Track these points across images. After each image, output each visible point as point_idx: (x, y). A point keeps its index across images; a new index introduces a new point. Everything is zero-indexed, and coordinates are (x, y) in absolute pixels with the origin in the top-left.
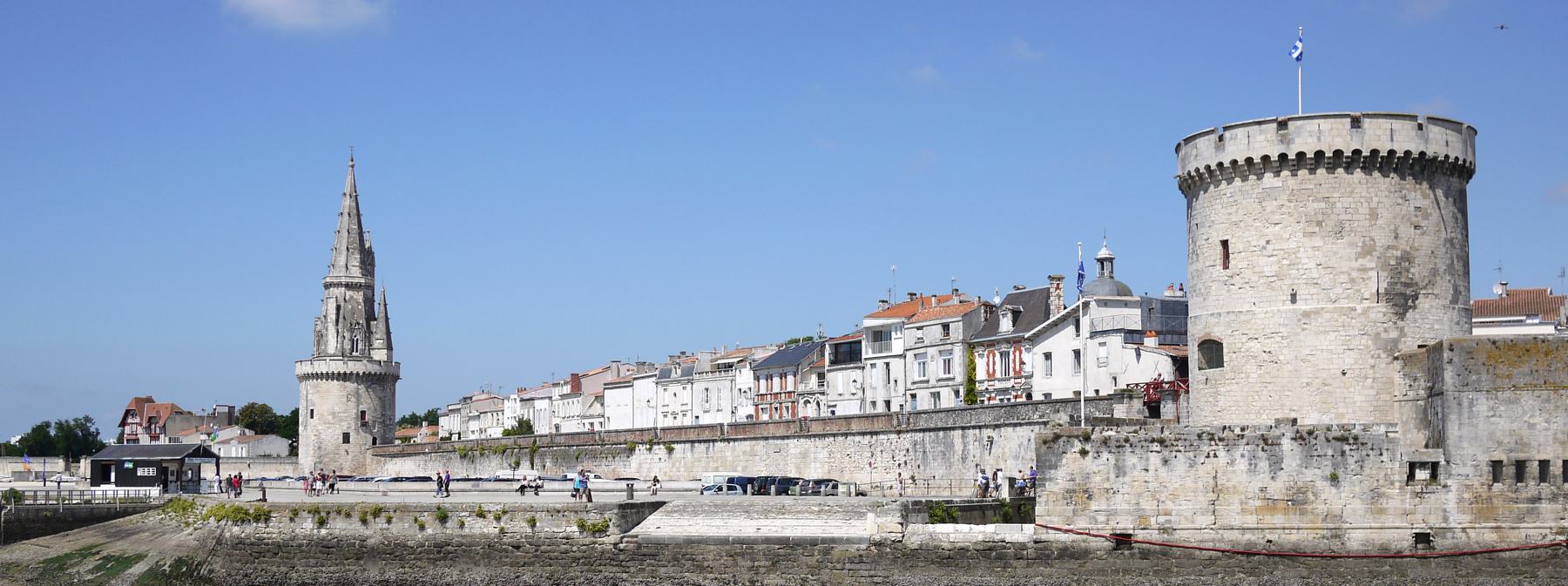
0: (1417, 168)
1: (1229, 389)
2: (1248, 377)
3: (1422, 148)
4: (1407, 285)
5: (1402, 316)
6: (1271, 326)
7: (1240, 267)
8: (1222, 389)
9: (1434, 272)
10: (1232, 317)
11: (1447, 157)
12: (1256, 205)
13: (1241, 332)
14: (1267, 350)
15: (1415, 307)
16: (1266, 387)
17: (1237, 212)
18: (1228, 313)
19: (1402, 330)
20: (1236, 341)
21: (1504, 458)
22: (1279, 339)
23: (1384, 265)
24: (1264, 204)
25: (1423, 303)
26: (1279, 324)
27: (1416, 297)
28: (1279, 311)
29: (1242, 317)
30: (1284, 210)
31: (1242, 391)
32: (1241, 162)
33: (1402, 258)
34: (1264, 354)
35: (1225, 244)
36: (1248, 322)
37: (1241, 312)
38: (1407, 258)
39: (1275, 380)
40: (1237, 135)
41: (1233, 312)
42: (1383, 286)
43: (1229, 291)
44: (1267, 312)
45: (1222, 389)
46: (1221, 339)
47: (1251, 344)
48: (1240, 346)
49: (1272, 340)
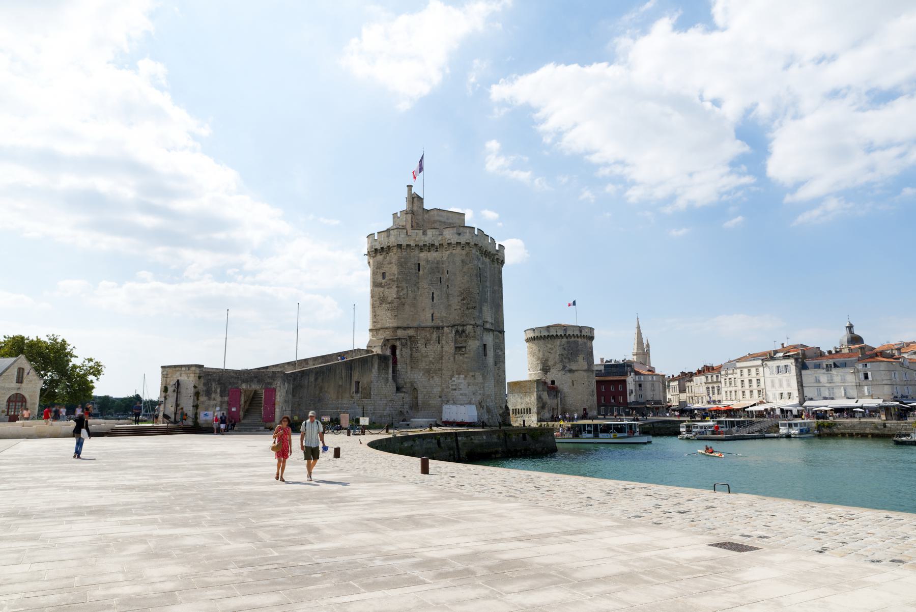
0: (549, 338)
3: (548, 334)
4: (546, 367)
5: (546, 374)
9: (555, 363)
11: (557, 335)
15: (550, 371)
19: (546, 377)
21: (513, 408)
23: (542, 363)
25: (552, 370)
27: (550, 369)
33: (546, 360)
38: (547, 360)
42: (541, 367)
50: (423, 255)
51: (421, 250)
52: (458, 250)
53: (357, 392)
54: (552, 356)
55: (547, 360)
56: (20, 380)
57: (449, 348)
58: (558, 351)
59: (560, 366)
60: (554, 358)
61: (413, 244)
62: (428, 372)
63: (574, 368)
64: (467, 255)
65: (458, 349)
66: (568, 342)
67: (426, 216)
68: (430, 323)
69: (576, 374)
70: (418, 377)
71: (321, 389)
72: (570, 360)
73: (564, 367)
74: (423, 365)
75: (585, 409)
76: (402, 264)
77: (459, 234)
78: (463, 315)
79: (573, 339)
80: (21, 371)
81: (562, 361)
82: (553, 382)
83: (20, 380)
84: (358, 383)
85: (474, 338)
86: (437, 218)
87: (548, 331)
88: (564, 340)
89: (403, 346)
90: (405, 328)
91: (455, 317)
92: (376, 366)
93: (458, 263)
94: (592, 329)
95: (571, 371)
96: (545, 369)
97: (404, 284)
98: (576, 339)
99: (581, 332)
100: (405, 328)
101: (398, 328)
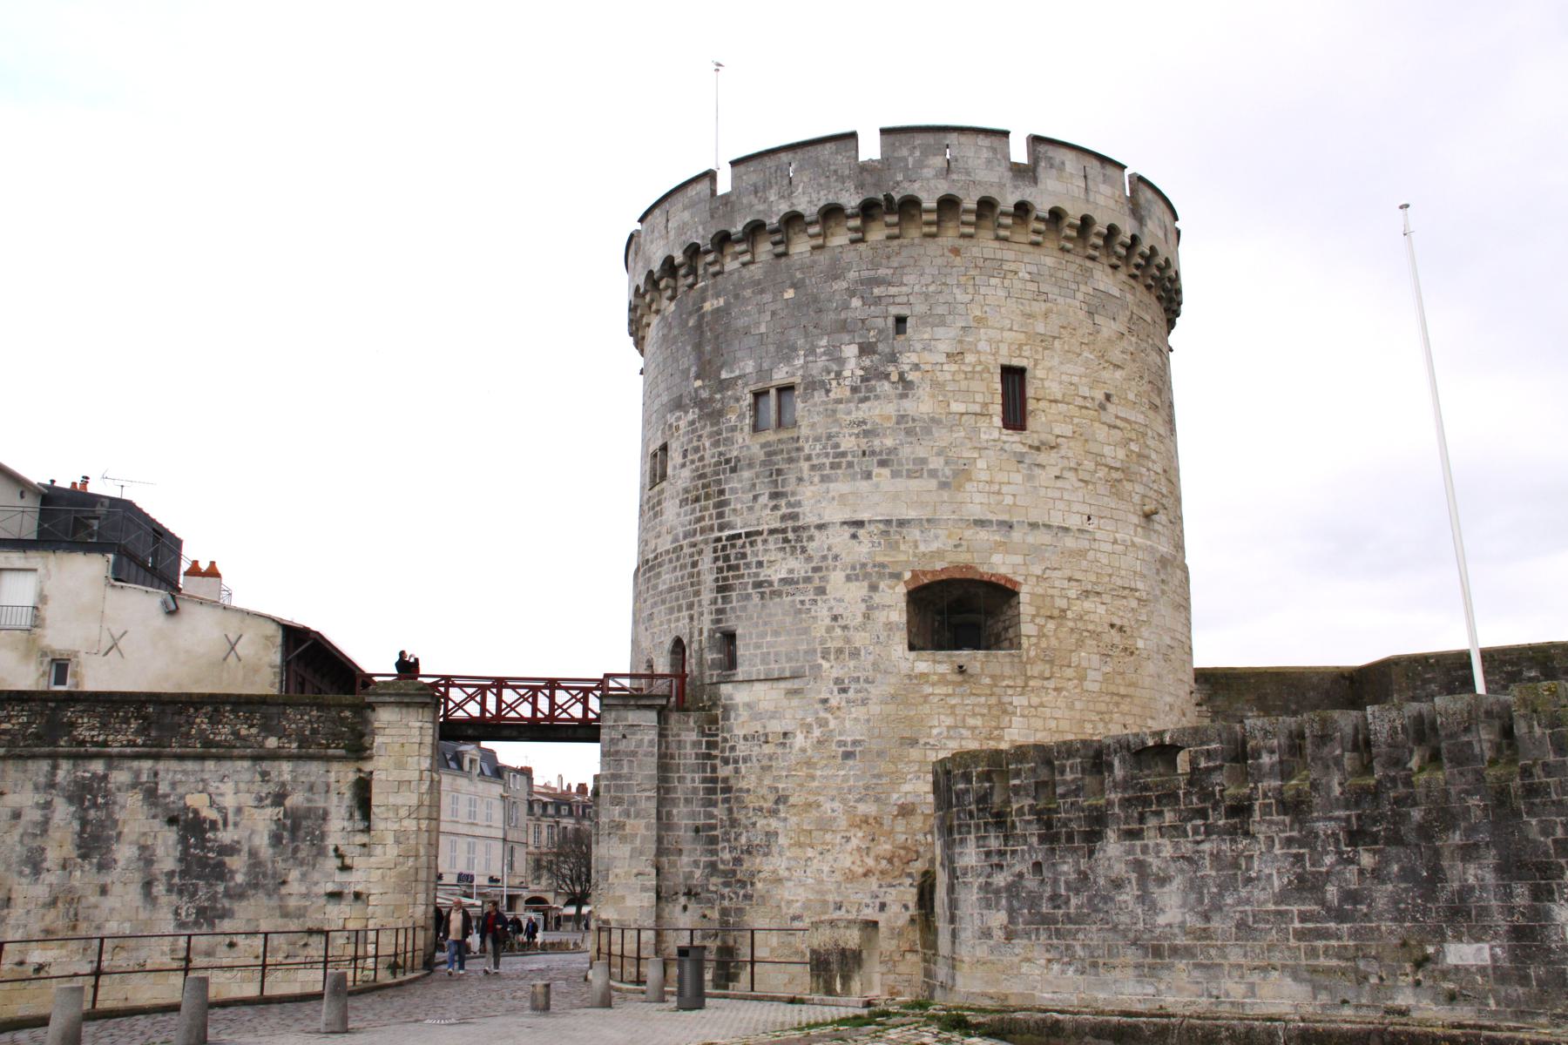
1: (1035, 700)
2: (1082, 678)
6: (1123, 573)
7: (1057, 431)
8: (1016, 701)
10: (1043, 537)
12: (1082, 315)
13: (1068, 573)
14: (1118, 622)
16: (1117, 704)
17: (1046, 315)
18: (1034, 526)
20: (1056, 592)
22: (1134, 604)
24: (1098, 319)
26: (1135, 572)
28: (1133, 544)
29: (1069, 542)
30: (1124, 344)
31: (1071, 707)
32: (1074, 213)
34: (1113, 632)
35: (1013, 377)
36: (1082, 553)
37: (1067, 530)
39: (1131, 690)
40: (1063, 163)
41: (1048, 526)
43: (1030, 478)
44: (1115, 542)
45: (1016, 701)
46: (1016, 583)
47: (1088, 605)
48: (1063, 603)
49: (1124, 602)
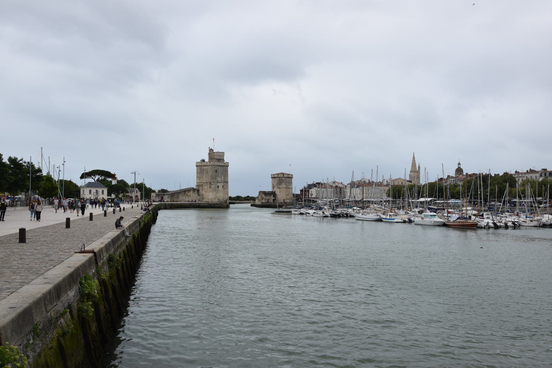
50: (204, 167)
51: (204, 166)
52: (210, 167)
53: (187, 196)
54: (275, 183)
55: (274, 185)
56: (137, 193)
57: (209, 187)
58: (276, 182)
59: (277, 186)
60: (275, 184)
61: (202, 165)
62: (205, 191)
63: (281, 187)
64: (212, 167)
65: (210, 187)
66: (279, 179)
67: (214, 154)
68: (205, 182)
69: (281, 189)
70: (203, 193)
71: (178, 195)
72: (279, 185)
73: (278, 187)
74: (204, 190)
75: (284, 200)
76: (200, 169)
77: (210, 163)
78: (211, 180)
79: (281, 178)
80: (137, 191)
81: (277, 185)
82: (275, 191)
83: (137, 193)
84: (187, 194)
85: (213, 185)
86: (217, 154)
87: (274, 175)
88: (278, 178)
89: (201, 186)
90: (201, 183)
91: (210, 181)
92: (192, 191)
93: (210, 169)
94: (292, 175)
95: (279, 188)
96: (273, 188)
97: (201, 174)
98: (282, 178)
99: (283, 176)
100: (201, 183)
101: (199, 183)
